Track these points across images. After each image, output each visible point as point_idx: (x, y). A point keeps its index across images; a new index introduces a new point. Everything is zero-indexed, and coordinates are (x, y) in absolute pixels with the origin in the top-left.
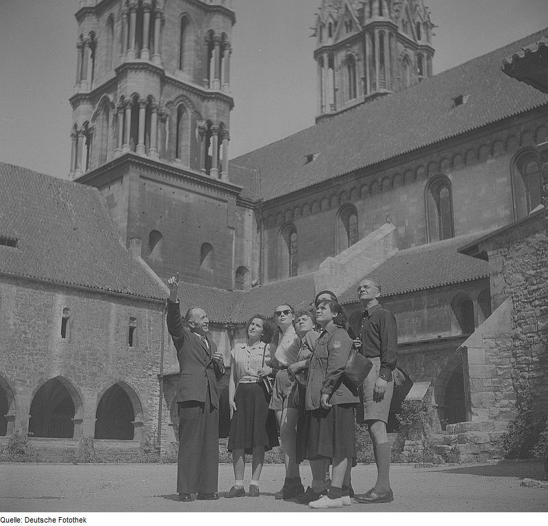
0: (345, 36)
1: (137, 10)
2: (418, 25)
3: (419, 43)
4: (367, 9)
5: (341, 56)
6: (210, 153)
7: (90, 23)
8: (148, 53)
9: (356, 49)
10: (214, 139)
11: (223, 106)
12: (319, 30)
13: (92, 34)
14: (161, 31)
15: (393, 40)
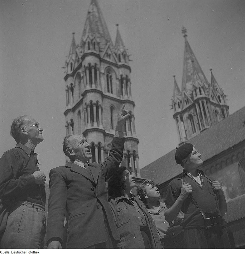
0: (186, 106)
1: (90, 106)
2: (219, 97)
3: (221, 104)
4: (194, 93)
5: (186, 115)
6: (131, 166)
7: (70, 116)
8: (97, 124)
9: (192, 111)
10: (131, 159)
11: (134, 143)
12: (174, 106)
13: (72, 120)
14: (102, 114)
15: (209, 104)
